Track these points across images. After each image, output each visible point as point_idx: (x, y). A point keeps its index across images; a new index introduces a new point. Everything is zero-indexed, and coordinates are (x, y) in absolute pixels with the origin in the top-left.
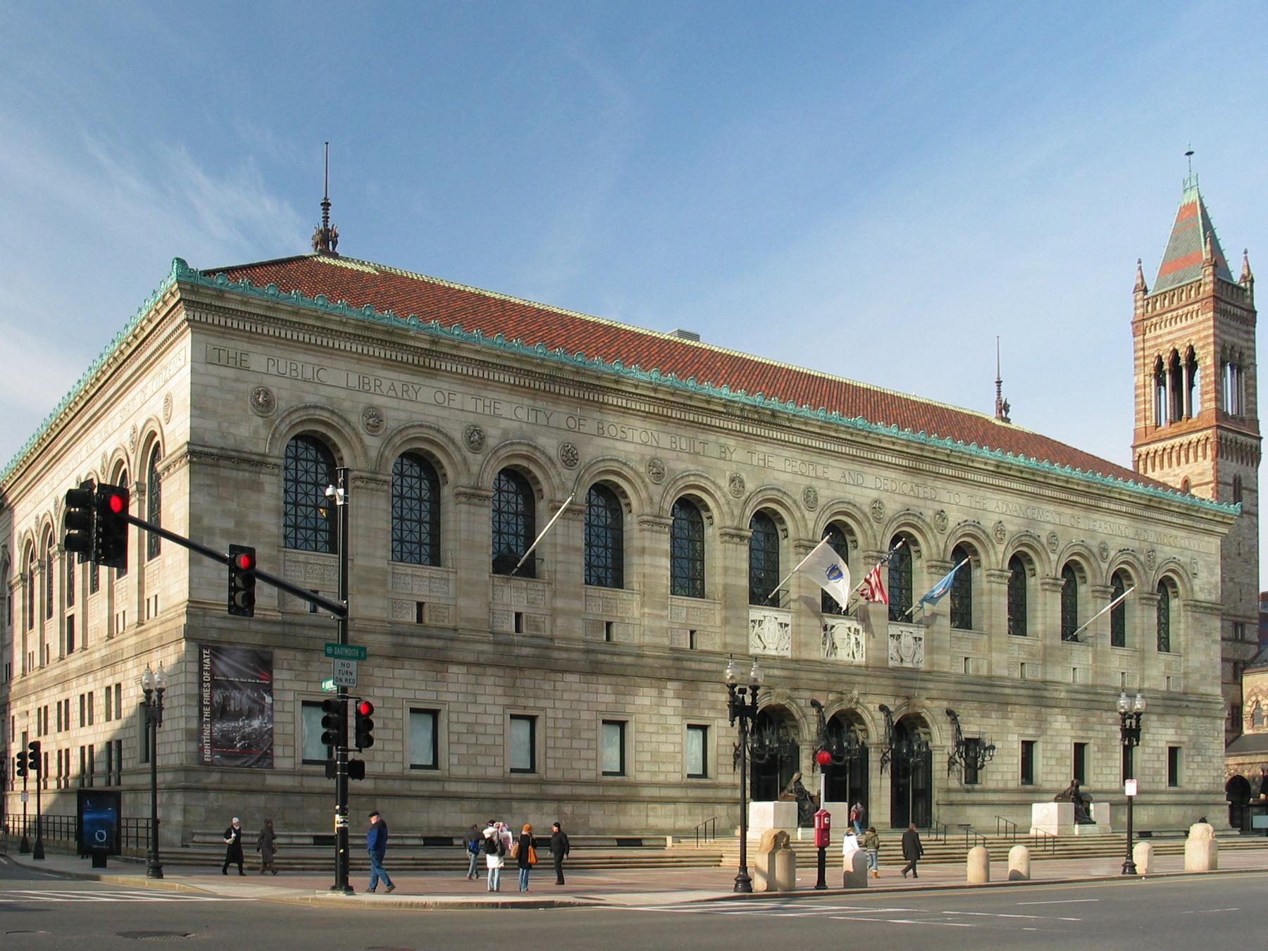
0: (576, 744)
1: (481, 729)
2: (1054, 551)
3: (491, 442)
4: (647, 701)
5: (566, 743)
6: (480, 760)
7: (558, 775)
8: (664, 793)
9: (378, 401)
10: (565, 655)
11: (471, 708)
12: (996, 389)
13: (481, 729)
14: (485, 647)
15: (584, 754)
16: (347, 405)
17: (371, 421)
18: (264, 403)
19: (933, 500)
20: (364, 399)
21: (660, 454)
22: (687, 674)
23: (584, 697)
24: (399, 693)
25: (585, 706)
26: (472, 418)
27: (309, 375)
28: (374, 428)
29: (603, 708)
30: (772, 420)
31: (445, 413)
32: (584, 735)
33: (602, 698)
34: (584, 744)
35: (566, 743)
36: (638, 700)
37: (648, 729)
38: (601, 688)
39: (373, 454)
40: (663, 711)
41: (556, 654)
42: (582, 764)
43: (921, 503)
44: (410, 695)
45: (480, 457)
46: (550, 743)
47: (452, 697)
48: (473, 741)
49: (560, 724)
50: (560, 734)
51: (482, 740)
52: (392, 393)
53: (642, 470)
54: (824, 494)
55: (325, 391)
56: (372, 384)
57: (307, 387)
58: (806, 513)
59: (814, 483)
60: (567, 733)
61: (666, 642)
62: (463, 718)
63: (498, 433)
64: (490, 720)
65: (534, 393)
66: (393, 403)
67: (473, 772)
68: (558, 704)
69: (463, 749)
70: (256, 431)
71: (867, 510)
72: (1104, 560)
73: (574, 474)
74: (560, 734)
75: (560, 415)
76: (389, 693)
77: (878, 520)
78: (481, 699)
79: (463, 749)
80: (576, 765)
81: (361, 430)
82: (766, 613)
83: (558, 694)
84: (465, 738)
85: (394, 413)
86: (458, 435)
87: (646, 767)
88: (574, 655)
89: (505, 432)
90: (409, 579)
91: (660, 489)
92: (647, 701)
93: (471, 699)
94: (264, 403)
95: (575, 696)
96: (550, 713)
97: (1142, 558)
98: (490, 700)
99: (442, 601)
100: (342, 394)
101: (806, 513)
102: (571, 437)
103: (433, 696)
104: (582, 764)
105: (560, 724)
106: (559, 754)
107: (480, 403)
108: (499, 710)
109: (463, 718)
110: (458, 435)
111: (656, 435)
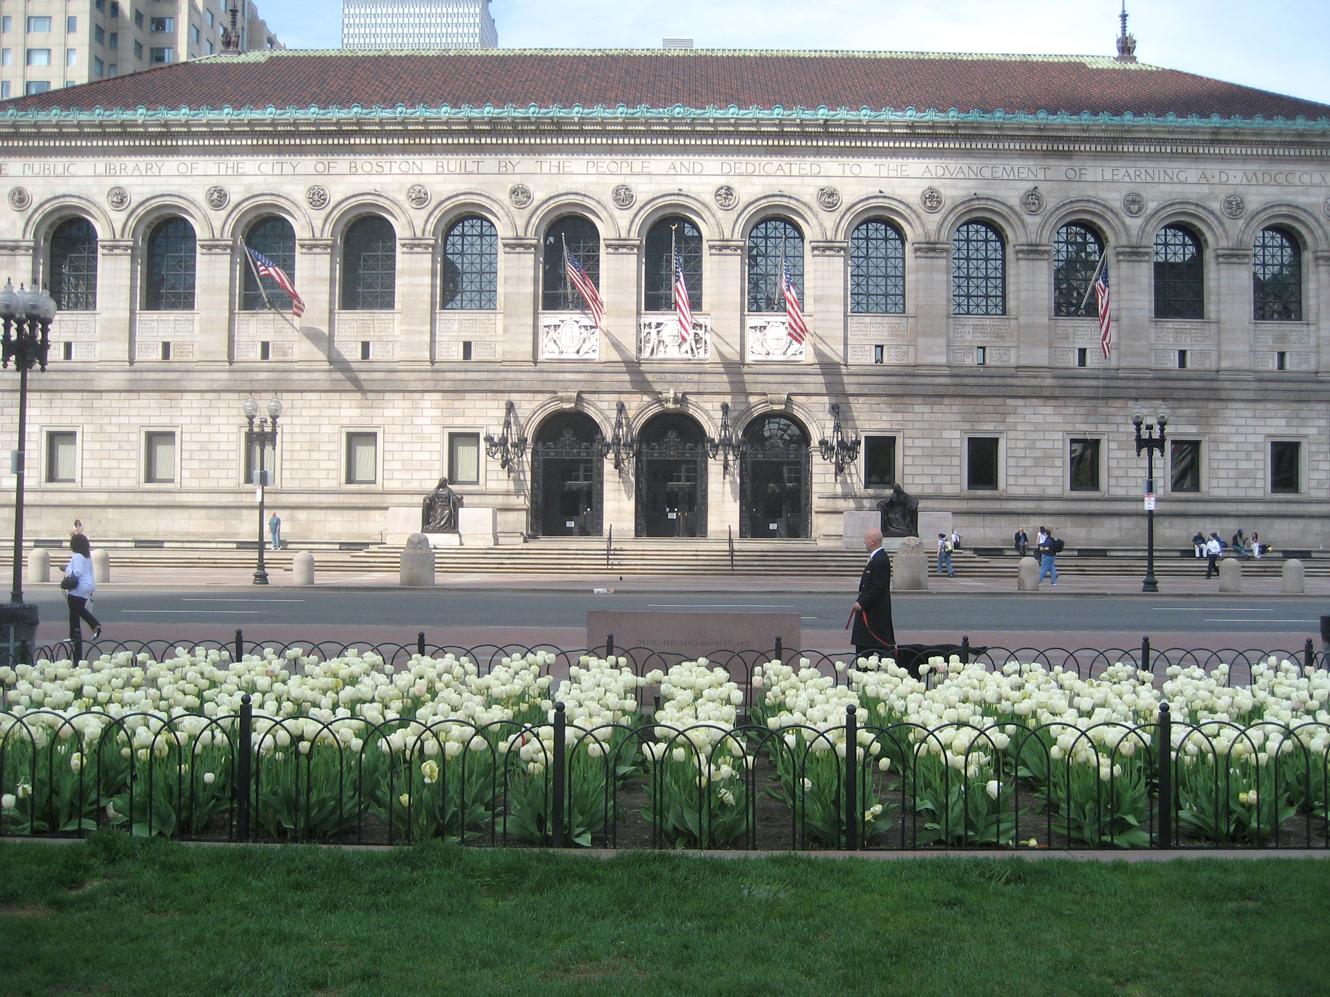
0: (315, 455)
1: (215, 447)
2: (1033, 213)
3: (234, 198)
4: (398, 413)
5: (304, 455)
6: (213, 473)
7: (295, 485)
8: (316, 499)
9: (122, 182)
10: (305, 376)
11: (205, 429)
13: (215, 447)
15: (324, 465)
16: (95, 190)
17: (115, 199)
18: (20, 198)
19: (817, 176)
20: (111, 182)
21: (422, 180)
22: (446, 386)
23: (325, 412)
24: (134, 420)
25: (326, 421)
26: (214, 181)
27: (60, 170)
29: (346, 421)
30: (558, 128)
31: (189, 180)
32: (324, 447)
33: (344, 412)
34: (324, 455)
35: (304, 455)
36: (387, 413)
37: (399, 438)
38: (346, 404)
40: (417, 421)
41: (295, 376)
42: (322, 474)
43: (797, 181)
44: (145, 421)
46: (286, 456)
47: (186, 420)
48: (206, 456)
49: (298, 438)
50: (297, 447)
51: (215, 455)
52: (137, 173)
55: (73, 181)
56: (118, 168)
57: (59, 181)
59: (629, 181)
60: (306, 446)
62: (196, 437)
63: (243, 188)
64: (224, 438)
65: (279, 150)
66: (139, 180)
67: (205, 484)
68: (295, 420)
69: (196, 465)
70: (14, 223)
72: (1133, 214)
73: (323, 213)
74: (297, 447)
75: (308, 163)
76: (125, 420)
77: (726, 208)
78: (215, 420)
79: (196, 465)
80: (314, 474)
82: (562, 317)
83: (297, 412)
84: (196, 455)
85: (138, 189)
87: (396, 475)
88: (316, 376)
89: (249, 186)
90: (155, 324)
91: (424, 214)
92: (398, 413)
93: (204, 420)
94: (20, 198)
95: (317, 413)
97: (1216, 206)
98: (224, 420)
99: (187, 339)
100: (90, 181)
102: (319, 181)
103: (166, 421)
104: (322, 474)
105: (298, 438)
106: (296, 465)
108: (235, 429)
109: (196, 437)
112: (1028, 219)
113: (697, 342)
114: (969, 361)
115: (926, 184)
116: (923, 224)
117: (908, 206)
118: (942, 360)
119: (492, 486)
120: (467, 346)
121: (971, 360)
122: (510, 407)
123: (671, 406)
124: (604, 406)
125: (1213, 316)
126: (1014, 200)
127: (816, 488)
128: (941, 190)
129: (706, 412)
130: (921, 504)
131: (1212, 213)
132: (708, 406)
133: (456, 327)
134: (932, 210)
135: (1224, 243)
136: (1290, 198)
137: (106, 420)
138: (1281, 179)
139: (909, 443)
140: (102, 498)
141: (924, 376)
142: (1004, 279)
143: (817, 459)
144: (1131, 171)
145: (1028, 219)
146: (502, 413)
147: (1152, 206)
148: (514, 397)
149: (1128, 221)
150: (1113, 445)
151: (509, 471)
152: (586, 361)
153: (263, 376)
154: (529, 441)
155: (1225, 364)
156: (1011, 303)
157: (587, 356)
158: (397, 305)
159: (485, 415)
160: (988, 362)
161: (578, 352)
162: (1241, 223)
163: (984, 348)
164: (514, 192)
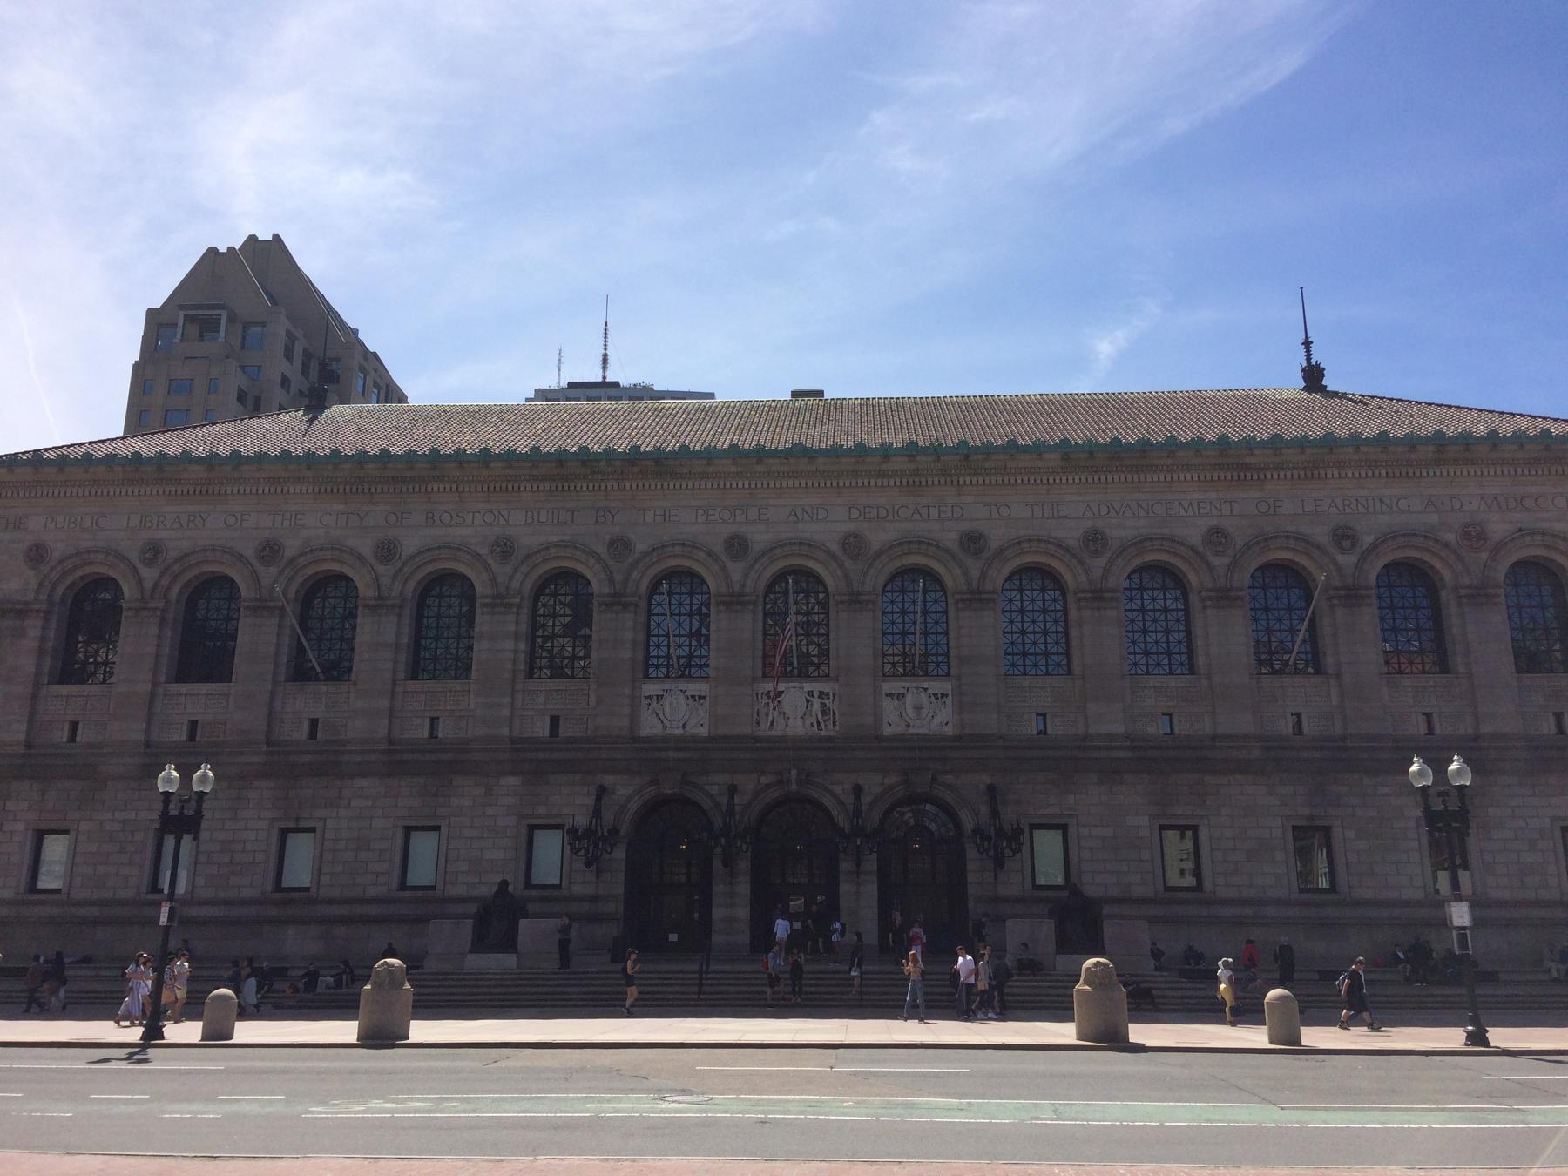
3: (289, 553)
9: (163, 534)
12: (1303, 352)
14: (256, 759)
28: (150, 563)
39: (148, 585)
45: (273, 570)
50: (341, 845)
53: (484, 551)
54: (760, 537)
58: (730, 565)
61: (505, 731)
68: (343, 812)
71: (834, 547)
74: (341, 845)
81: (138, 565)
82: (666, 687)
86: (249, 553)
96: (330, 824)
97: (1450, 537)
101: (730, 565)
107: (279, 519)
110: (249, 553)
111: (505, 513)
112: (1217, 561)
113: (824, 713)
114: (1151, 730)
115: (1089, 524)
116: (1086, 571)
117: (1067, 550)
118: (1121, 730)
119: (577, 889)
120: (555, 721)
121: (1157, 729)
122: (602, 791)
123: (794, 787)
124: (714, 790)
125: (1461, 669)
126: (1195, 539)
127: (971, 890)
128: (1107, 531)
129: (835, 796)
130: (1106, 910)
131: (1446, 545)
132: (838, 789)
133: (542, 699)
134: (1097, 553)
135: (1467, 581)
136: (1545, 525)
137: (109, 816)
138: (1528, 503)
139: (1084, 831)
140: (95, 911)
141: (1099, 748)
142: (1189, 633)
143: (971, 853)
144: (1339, 501)
145: (1217, 561)
146: (590, 801)
147: (1368, 540)
148: (609, 780)
149: (1340, 558)
150: (1351, 834)
151: (598, 872)
152: (695, 739)
153: (307, 758)
154: (623, 832)
155: (1486, 729)
156: (1201, 660)
157: (694, 731)
158: (474, 674)
159: (571, 801)
160: (1176, 731)
161: (684, 726)
162: (1484, 556)
163: (1170, 715)
164: (612, 543)
